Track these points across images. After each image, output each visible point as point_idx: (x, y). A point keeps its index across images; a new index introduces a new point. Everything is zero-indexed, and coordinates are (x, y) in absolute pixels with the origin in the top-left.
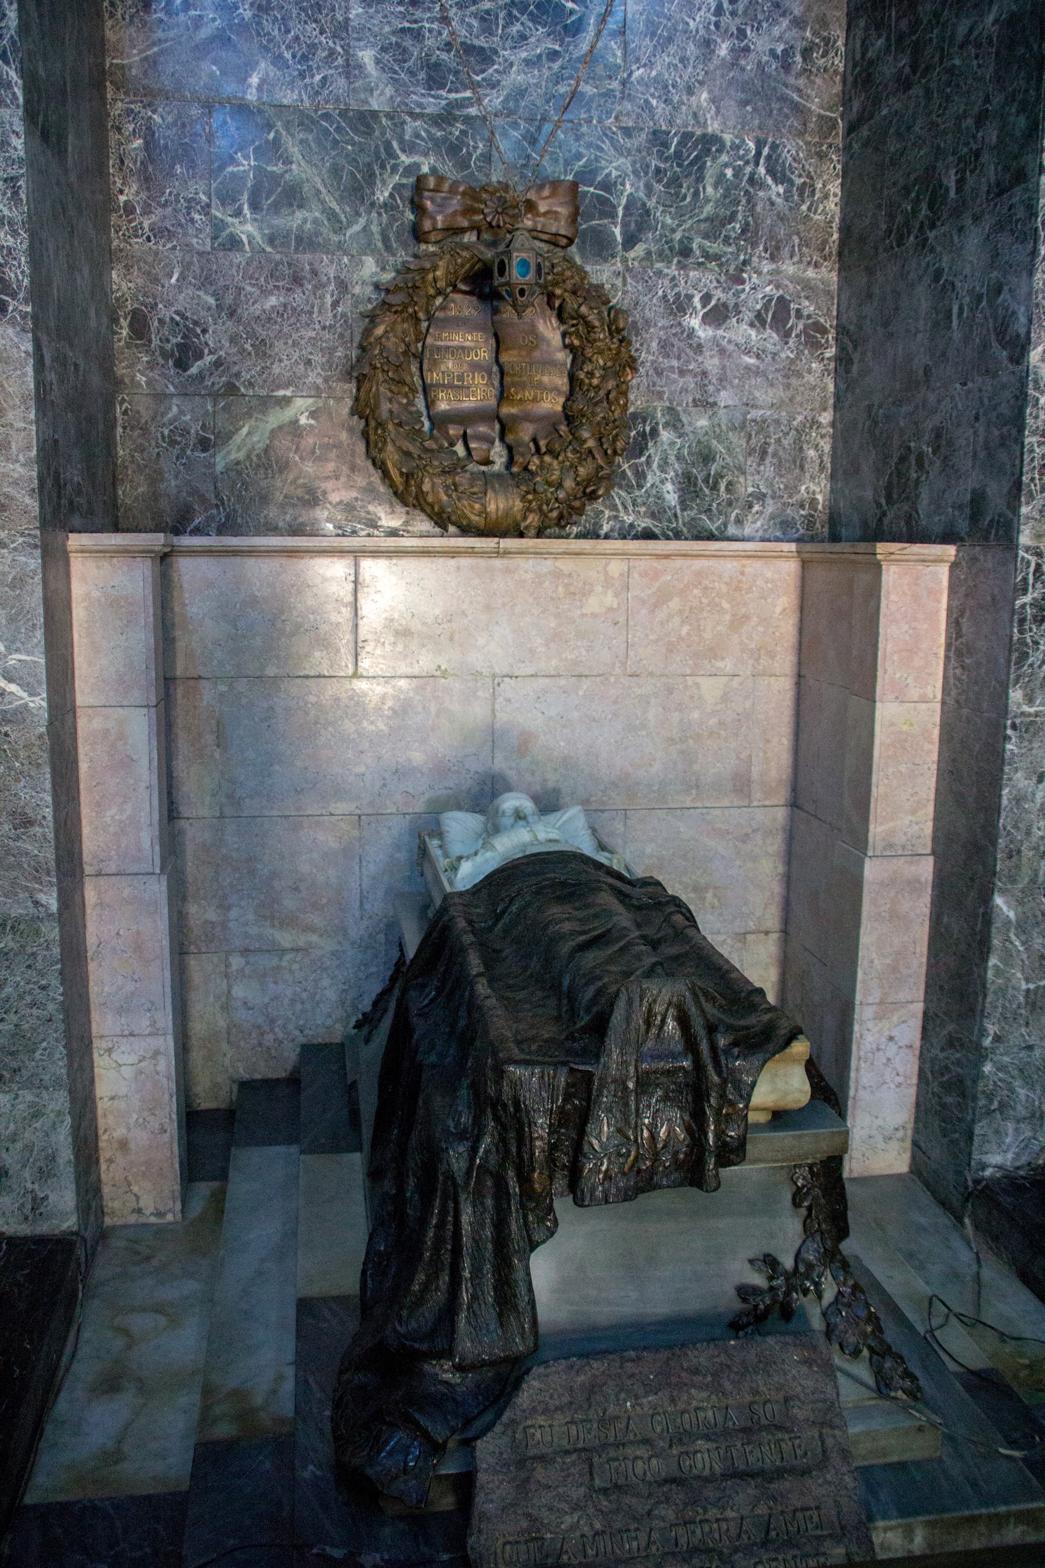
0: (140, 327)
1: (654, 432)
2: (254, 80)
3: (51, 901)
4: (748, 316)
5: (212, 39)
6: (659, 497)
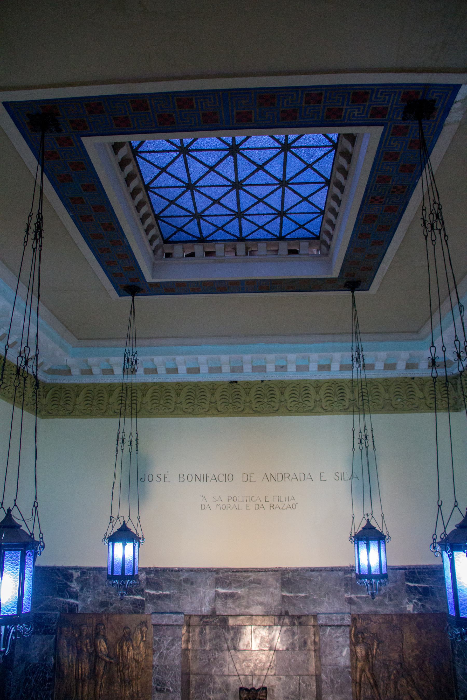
2: (213, 671)
5: (206, 665)
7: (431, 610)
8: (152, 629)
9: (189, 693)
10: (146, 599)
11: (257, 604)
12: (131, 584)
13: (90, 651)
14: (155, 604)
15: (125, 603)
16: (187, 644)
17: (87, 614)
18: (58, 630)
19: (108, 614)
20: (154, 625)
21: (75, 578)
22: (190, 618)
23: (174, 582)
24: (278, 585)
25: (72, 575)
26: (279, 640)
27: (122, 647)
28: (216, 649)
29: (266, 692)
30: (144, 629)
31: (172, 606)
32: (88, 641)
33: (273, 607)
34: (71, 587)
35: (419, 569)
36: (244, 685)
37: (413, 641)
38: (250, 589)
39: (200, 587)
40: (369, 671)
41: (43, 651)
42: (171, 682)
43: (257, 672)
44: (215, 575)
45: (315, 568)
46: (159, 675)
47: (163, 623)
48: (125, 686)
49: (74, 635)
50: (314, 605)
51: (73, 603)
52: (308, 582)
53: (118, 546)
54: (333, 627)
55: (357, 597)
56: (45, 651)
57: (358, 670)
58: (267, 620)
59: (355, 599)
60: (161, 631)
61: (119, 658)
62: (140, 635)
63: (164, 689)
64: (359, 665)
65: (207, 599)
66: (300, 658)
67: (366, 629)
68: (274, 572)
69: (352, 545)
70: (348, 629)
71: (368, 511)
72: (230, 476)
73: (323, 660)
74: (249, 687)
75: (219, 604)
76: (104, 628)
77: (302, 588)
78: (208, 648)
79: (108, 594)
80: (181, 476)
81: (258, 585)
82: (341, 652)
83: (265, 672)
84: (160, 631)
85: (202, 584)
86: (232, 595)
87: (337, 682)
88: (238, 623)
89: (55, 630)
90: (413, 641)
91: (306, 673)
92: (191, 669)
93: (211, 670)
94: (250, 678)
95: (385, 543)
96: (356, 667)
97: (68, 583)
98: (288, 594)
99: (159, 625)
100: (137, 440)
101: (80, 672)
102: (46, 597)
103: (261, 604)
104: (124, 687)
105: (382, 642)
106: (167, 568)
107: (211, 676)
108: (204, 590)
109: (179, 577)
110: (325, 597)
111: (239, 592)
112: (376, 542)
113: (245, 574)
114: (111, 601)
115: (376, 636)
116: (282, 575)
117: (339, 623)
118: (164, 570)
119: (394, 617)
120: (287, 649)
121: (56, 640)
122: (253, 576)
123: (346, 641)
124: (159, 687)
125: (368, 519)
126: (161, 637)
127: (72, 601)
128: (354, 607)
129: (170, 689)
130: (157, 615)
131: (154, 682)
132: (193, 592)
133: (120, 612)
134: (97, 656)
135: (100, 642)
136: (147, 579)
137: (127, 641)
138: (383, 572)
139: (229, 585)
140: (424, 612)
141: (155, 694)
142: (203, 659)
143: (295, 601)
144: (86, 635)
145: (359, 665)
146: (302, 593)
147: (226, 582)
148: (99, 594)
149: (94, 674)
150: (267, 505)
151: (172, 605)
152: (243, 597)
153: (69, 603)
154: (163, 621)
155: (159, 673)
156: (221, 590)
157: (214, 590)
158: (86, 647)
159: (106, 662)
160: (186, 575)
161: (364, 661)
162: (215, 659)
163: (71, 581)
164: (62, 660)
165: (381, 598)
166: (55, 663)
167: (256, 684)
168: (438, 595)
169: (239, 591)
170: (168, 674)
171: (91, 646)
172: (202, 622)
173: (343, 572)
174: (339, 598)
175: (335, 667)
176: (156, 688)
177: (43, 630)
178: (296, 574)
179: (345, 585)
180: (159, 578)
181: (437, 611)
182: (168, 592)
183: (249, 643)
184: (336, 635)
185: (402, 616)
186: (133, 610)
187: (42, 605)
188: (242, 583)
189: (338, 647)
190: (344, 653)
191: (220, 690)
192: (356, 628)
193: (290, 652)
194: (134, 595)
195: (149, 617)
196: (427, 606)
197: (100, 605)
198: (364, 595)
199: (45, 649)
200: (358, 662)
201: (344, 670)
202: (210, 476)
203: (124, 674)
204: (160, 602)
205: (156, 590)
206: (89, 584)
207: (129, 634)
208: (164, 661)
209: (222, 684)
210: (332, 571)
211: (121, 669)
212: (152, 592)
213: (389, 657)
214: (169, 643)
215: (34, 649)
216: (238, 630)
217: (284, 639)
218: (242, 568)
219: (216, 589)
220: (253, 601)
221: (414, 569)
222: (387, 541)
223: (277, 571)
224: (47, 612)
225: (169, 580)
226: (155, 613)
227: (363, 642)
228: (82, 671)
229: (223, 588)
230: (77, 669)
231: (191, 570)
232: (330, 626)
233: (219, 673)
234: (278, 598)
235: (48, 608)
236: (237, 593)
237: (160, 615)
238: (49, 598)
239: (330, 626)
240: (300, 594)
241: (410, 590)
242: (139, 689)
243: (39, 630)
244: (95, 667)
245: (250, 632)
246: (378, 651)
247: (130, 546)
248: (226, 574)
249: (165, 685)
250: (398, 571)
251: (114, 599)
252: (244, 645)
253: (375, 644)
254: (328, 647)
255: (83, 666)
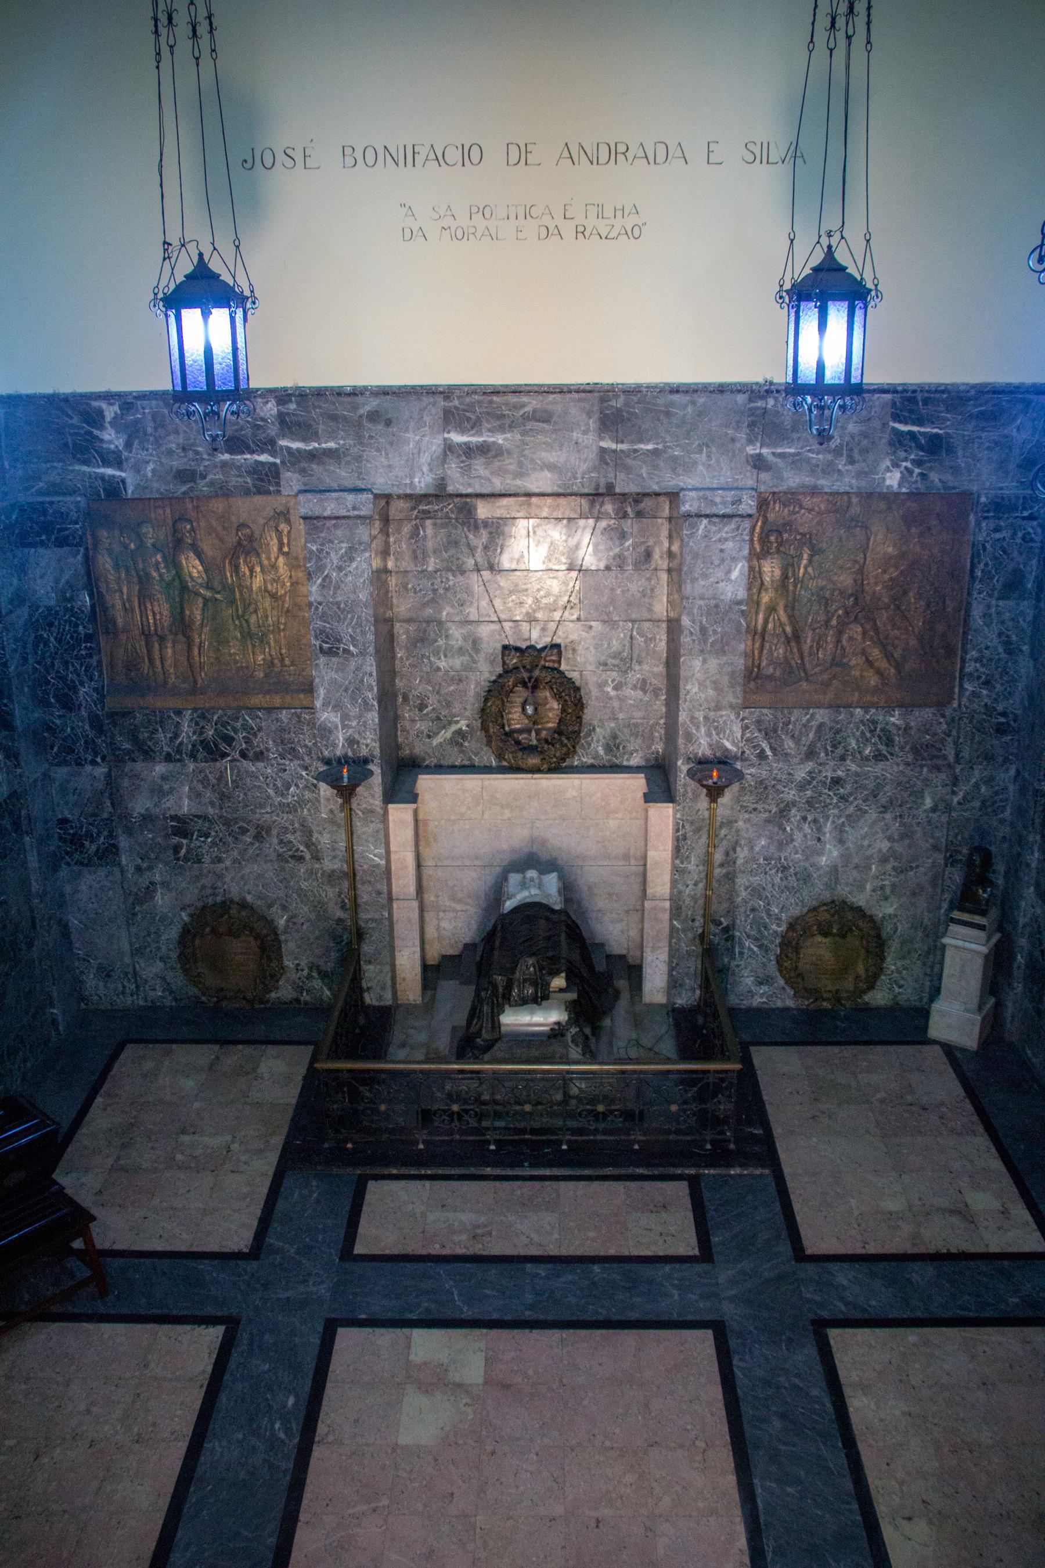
0: (406, 698)
1: (594, 729)
2: (444, 613)
3: (386, 914)
4: (630, 686)
5: (428, 601)
6: (597, 752)
7: (939, 485)
8: (301, 527)
9: (394, 658)
10: (283, 462)
11: (542, 469)
12: (233, 413)
13: (168, 577)
14: (303, 471)
15: (234, 472)
16: (385, 560)
17: (149, 499)
18: (89, 537)
19: (198, 498)
20: (305, 518)
21: (108, 419)
22: (388, 503)
23: (345, 418)
24: (592, 424)
25: (100, 413)
26: (591, 548)
27: (236, 568)
28: (449, 569)
29: (560, 654)
30: (284, 527)
31: (344, 475)
32: (159, 557)
33: (579, 475)
34: (102, 441)
35: (928, 391)
36: (511, 641)
37: (890, 550)
38: (524, 433)
39: (407, 430)
40: (785, 611)
41: (63, 581)
42: (351, 636)
43: (539, 615)
44: (442, 403)
45: (679, 385)
46: (325, 621)
47: (327, 513)
48: (254, 646)
49: (126, 546)
50: (674, 470)
51: (114, 476)
52: (662, 417)
53: (191, 317)
54: (714, 519)
55: (774, 454)
56: (67, 582)
57: (763, 608)
58: (566, 507)
59: (771, 458)
60: (321, 532)
61: (233, 591)
62: (275, 541)
63: (338, 649)
64: (765, 598)
65: (425, 458)
66: (636, 586)
67: (788, 525)
68: (583, 395)
69: (782, 314)
70: (747, 524)
71: (832, 222)
72: (475, 151)
73: (688, 589)
74: (524, 646)
75: (453, 469)
76: (193, 529)
77: (647, 431)
78: (432, 564)
79: (191, 454)
80: (348, 151)
81: (545, 426)
82: (729, 571)
83: (557, 615)
84: (316, 528)
85: (412, 424)
86: (484, 449)
87: (715, 632)
88: (499, 513)
89: (81, 538)
90: (890, 550)
91: (647, 616)
92: (395, 610)
93: (440, 612)
94: (525, 627)
95: (866, 308)
96: (758, 603)
97: (96, 432)
98: (613, 446)
99: (317, 518)
100: (209, 17)
101: (151, 621)
102: (48, 465)
103: (551, 467)
104: (250, 646)
105: (821, 551)
106: (326, 388)
107: (440, 623)
108: (417, 438)
109: (355, 407)
110: (701, 452)
111: (500, 442)
112: (845, 304)
113: (513, 399)
114: (202, 468)
115: (808, 540)
116: (603, 400)
117: (728, 510)
118: (320, 393)
119: (855, 500)
120: (608, 568)
121: (86, 556)
122: (532, 403)
123: (740, 549)
124: (325, 645)
125: (830, 247)
126: (322, 545)
127: (110, 471)
128: (763, 476)
129: (352, 648)
130: (309, 496)
131: (316, 637)
132: (391, 444)
133: (223, 492)
134: (184, 588)
135: (187, 559)
136: (281, 418)
137: (247, 554)
138: (853, 381)
139: (475, 425)
140: (923, 490)
141: (319, 658)
142: (421, 590)
143: (629, 462)
144: (154, 545)
145: (765, 598)
146: (649, 441)
147: (468, 419)
148: (170, 453)
149: (182, 625)
150: (568, 229)
151: (343, 474)
152: (509, 452)
153: (102, 477)
154: (325, 509)
155: (323, 617)
156: (457, 438)
157: (441, 437)
158: (158, 569)
159: (206, 601)
160: (371, 404)
161: (776, 590)
162: (447, 589)
163: (102, 428)
164: (108, 597)
165: (829, 457)
166: (93, 606)
167: (538, 638)
168: (960, 453)
169: (500, 439)
170: (345, 619)
171: (167, 567)
172: (415, 512)
173: (746, 395)
174: (734, 456)
175: (713, 602)
176: (321, 648)
177: (53, 537)
178: (635, 399)
179: (749, 426)
180: (309, 412)
181: (954, 488)
182: (332, 445)
183: (522, 556)
184: (719, 536)
185: (872, 497)
186: (255, 486)
187: (41, 484)
188: (507, 421)
189: (723, 560)
190: (735, 574)
191: (461, 651)
192: (764, 523)
193: (613, 574)
194: (252, 452)
195: (292, 503)
196: (934, 477)
197: (175, 477)
198: (792, 450)
199: (66, 577)
200: (763, 594)
201: (730, 608)
202: (423, 152)
203: (247, 621)
204: (314, 466)
205: (304, 440)
206: (145, 433)
207: (251, 539)
208: (335, 593)
209: (465, 639)
210: (722, 392)
211: (240, 612)
212: (295, 445)
213: (833, 583)
214: (342, 556)
215: (41, 577)
216: (497, 530)
217: (601, 547)
218: (507, 386)
219: (446, 435)
220: (533, 461)
221: (914, 391)
222: (872, 303)
223: (590, 392)
224: (55, 499)
225: (334, 418)
226: (305, 491)
227: (778, 551)
228: (155, 619)
229: (463, 431)
230: (143, 614)
231: (384, 392)
232: (707, 516)
233: (457, 619)
234: (591, 455)
235: (57, 489)
236: (494, 443)
237: (318, 496)
238: (55, 468)
239: (707, 516)
240: (642, 446)
241: (899, 441)
242: (284, 651)
243: (44, 537)
244: (182, 612)
245: (524, 532)
246: (810, 570)
247: (220, 316)
248: (468, 400)
249: (339, 640)
250: (877, 396)
251: (207, 463)
252: (512, 560)
253: (805, 556)
254: (699, 561)
255: (156, 609)
